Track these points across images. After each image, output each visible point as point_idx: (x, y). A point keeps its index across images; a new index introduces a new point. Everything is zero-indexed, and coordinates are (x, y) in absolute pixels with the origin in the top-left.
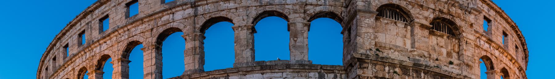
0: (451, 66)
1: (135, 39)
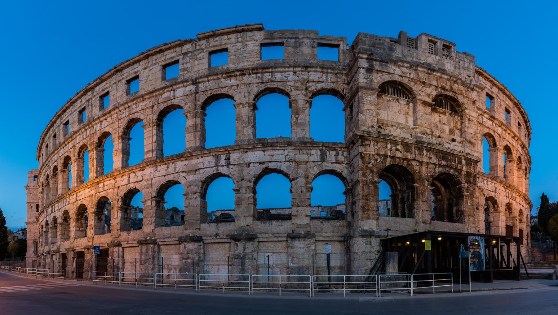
0: (454, 143)
1: (136, 116)
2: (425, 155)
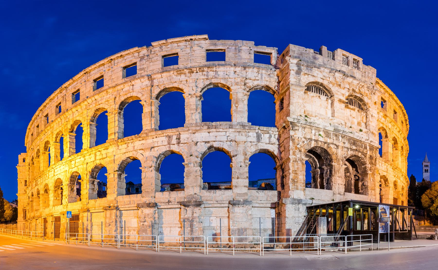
2: (340, 140)
